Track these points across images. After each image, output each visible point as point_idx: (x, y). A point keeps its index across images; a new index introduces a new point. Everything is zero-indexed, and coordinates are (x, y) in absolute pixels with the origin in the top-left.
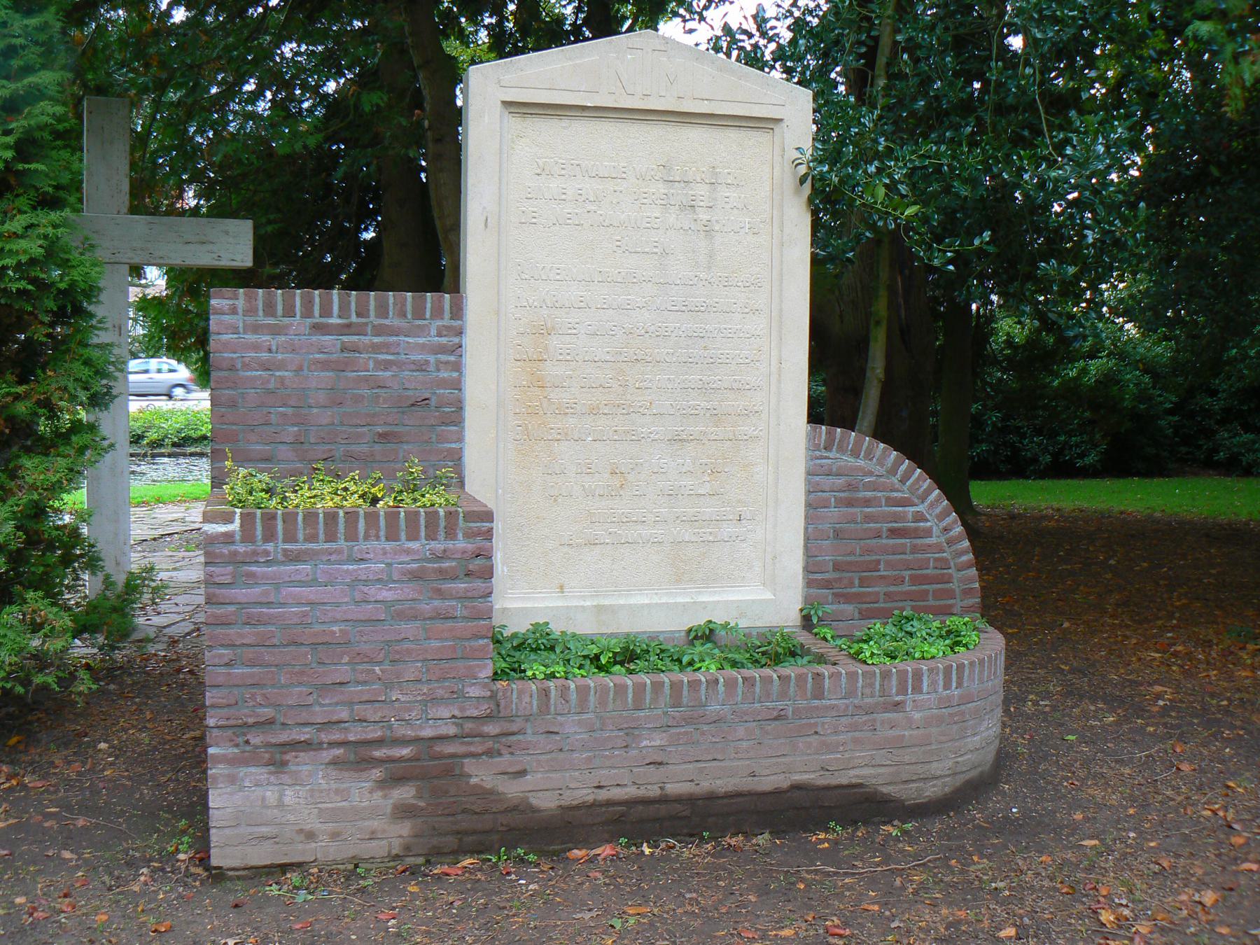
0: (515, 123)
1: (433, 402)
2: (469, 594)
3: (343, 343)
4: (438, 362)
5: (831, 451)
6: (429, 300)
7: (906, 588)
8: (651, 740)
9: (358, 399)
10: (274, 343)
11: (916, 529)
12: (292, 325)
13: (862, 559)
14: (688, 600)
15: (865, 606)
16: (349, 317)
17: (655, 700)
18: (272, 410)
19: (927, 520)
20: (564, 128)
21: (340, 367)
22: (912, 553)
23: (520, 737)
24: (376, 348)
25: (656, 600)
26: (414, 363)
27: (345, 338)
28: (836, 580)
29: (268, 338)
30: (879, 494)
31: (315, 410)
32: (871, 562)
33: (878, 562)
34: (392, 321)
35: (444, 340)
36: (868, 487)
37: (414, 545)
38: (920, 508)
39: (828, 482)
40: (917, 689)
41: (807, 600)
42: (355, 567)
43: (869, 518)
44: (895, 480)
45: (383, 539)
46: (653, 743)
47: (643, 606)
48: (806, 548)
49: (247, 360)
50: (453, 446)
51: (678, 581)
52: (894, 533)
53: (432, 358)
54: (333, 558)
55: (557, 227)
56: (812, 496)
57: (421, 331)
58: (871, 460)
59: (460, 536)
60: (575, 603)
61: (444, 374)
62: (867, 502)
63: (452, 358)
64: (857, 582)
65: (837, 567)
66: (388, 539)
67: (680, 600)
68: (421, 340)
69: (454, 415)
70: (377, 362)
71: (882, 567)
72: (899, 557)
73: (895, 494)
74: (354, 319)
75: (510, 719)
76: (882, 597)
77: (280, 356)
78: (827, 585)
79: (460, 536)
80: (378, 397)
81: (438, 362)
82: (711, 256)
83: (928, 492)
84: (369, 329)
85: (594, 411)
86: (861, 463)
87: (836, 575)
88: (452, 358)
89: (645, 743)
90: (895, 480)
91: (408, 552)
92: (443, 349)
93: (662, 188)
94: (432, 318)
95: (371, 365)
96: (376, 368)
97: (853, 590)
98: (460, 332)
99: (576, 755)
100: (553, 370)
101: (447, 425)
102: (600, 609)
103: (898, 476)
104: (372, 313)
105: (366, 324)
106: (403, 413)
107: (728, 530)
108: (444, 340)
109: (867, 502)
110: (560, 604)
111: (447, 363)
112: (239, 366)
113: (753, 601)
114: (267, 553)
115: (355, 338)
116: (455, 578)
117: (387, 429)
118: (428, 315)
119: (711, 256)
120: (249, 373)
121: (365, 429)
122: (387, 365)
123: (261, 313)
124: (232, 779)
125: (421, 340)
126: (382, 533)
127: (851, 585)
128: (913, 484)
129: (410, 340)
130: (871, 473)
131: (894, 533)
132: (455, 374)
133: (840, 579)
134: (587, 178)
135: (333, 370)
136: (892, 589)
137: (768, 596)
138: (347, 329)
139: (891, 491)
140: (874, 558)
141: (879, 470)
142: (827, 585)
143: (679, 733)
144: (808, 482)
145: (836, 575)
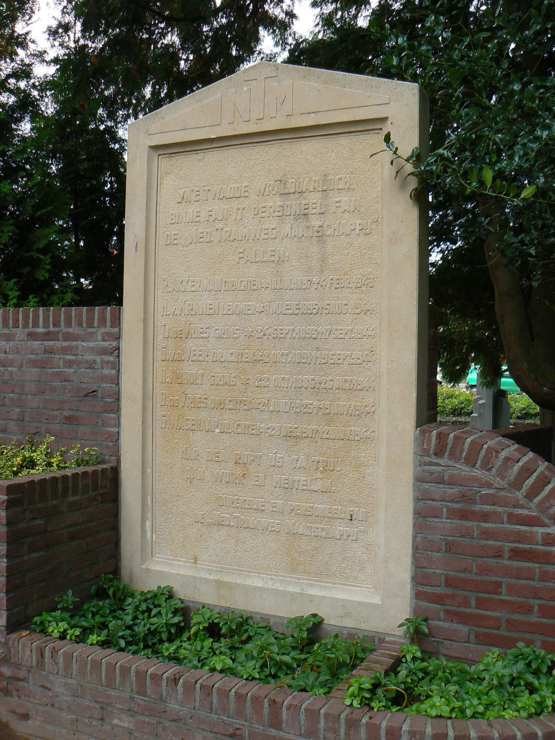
0: (166, 163)
1: (100, 393)
3: (45, 346)
4: (103, 362)
5: (442, 456)
6: (96, 313)
7: (535, 618)
8: (121, 720)
9: (53, 390)
10: (7, 347)
11: (547, 554)
12: (17, 333)
13: (478, 578)
14: (297, 590)
15: (483, 630)
16: (49, 327)
17: (123, 683)
18: (6, 395)
20: (200, 160)
21: (43, 364)
22: (541, 579)
24: (65, 351)
25: (270, 585)
26: (86, 362)
27: (46, 343)
28: (448, 596)
29: (4, 343)
30: (500, 509)
31: (29, 397)
32: (490, 582)
33: (499, 584)
34: (74, 330)
35: (106, 344)
36: (486, 499)
39: (438, 490)
41: (416, 611)
43: (486, 534)
44: (520, 495)
46: (122, 724)
47: (255, 589)
48: (414, 555)
50: (113, 429)
51: (293, 571)
52: (516, 554)
53: (98, 359)
55: (193, 245)
56: (421, 503)
57: (91, 337)
58: (489, 470)
60: (202, 575)
61: (106, 372)
62: (485, 517)
63: (111, 359)
64: (473, 603)
65: (450, 582)
67: (290, 589)
68: (91, 344)
69: (114, 405)
70: (65, 361)
71: (504, 589)
72: (524, 582)
73: (520, 511)
74: (51, 328)
75: (18, 666)
76: (504, 623)
77: (10, 357)
78: (438, 599)
80: (65, 388)
81: (103, 362)
82: (323, 260)
84: (60, 336)
85: (220, 406)
86: (478, 472)
87: (449, 591)
88: (111, 359)
89: (116, 721)
90: (520, 495)
92: (104, 352)
93: (278, 201)
94: (98, 327)
96: (64, 367)
97: (469, 610)
98: (118, 338)
99: (63, 714)
100: (189, 369)
101: (109, 412)
102: (220, 584)
104: (62, 324)
105: (58, 332)
106: (81, 401)
107: (340, 528)
108: (106, 344)
109: (485, 517)
110: (190, 573)
111: (108, 362)
113: (359, 603)
115: (52, 343)
117: (71, 413)
118: (96, 324)
119: (323, 260)
121: (58, 413)
122: (69, 364)
125: (91, 344)
127: (466, 603)
128: (542, 502)
129: (85, 344)
130: (489, 485)
131: (516, 554)
132: (113, 372)
133: (453, 596)
134: (216, 201)
135: (39, 367)
136: (516, 617)
137: (376, 600)
138: (47, 336)
139: (515, 506)
140: (494, 579)
141: (499, 482)
142: (438, 599)
143: (144, 722)
144: (416, 488)
145: (449, 591)
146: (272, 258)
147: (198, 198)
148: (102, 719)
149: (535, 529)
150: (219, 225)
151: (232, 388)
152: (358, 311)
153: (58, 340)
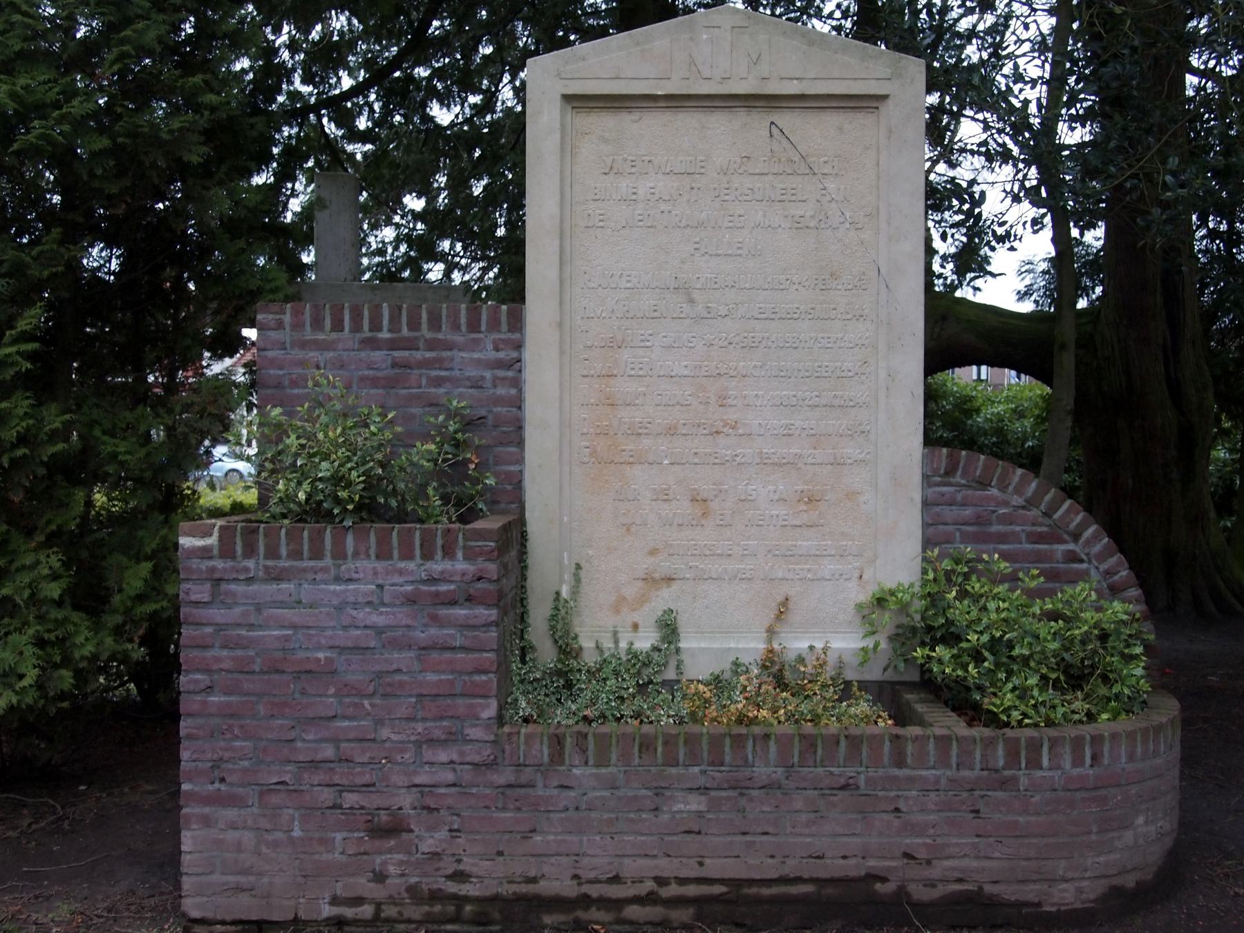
2: (471, 622)
3: (394, 358)
4: (495, 380)
16: (400, 331)
19: (1082, 561)
23: (530, 791)
26: (468, 378)
27: (396, 354)
30: (1018, 529)
36: (1004, 520)
37: (412, 565)
38: (1071, 546)
39: (950, 513)
40: (1035, 763)
42: (343, 587)
45: (373, 557)
49: (294, 376)
50: (512, 468)
53: (488, 375)
54: (318, 577)
56: (931, 530)
57: (475, 345)
59: (460, 555)
61: (501, 391)
66: (378, 557)
68: (476, 355)
70: (429, 378)
79: (460, 555)
83: (1083, 527)
85: (671, 431)
88: (510, 374)
91: (401, 572)
92: (500, 365)
95: (424, 382)
96: (429, 385)
98: (519, 346)
99: (593, 815)
103: (1043, 507)
104: (424, 326)
105: (416, 338)
108: (501, 355)
111: (504, 379)
112: (286, 383)
114: (247, 570)
116: (453, 603)
118: (483, 328)
120: (296, 391)
122: (438, 382)
123: (308, 328)
124: (206, 821)
125: (476, 355)
126: (372, 552)
129: (465, 355)
132: (513, 391)
134: (660, 176)
135: (383, 387)
146: (739, 252)
147: (633, 170)
148: (656, 809)
149: (1056, 547)
150: (663, 207)
151: (685, 408)
152: (849, 317)
153: (418, 349)
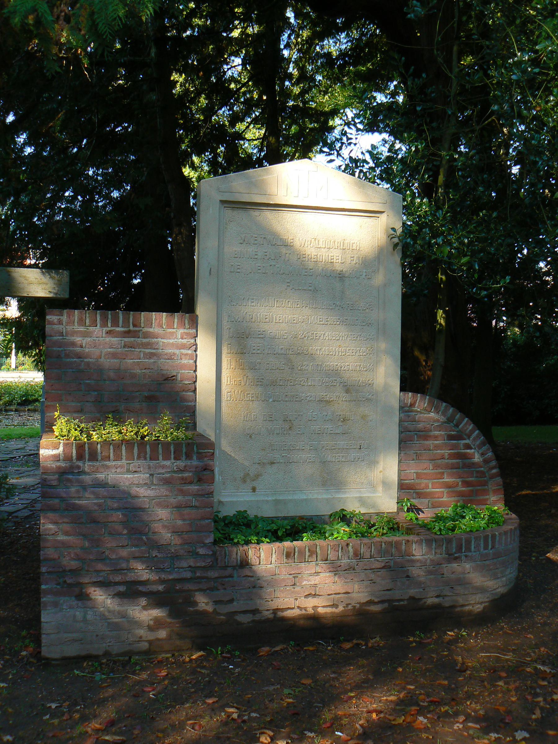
0: (229, 213)
2: (200, 493)
3: (125, 342)
8: (308, 580)
10: (84, 342)
12: (95, 331)
16: (129, 327)
19: (471, 448)
23: (230, 579)
29: (80, 339)
31: (107, 382)
35: (185, 341)
37: (167, 463)
38: (467, 441)
40: (468, 549)
42: (131, 476)
45: (148, 459)
49: (67, 352)
54: (118, 470)
56: (403, 434)
59: (195, 458)
60: (262, 498)
63: (189, 352)
64: (430, 486)
66: (151, 459)
70: (145, 354)
74: (131, 328)
79: (195, 458)
83: (472, 432)
84: (140, 334)
88: (189, 352)
91: (163, 467)
95: (142, 355)
102: (277, 502)
103: (454, 422)
108: (185, 341)
110: (253, 499)
111: (187, 354)
112: (63, 356)
114: (79, 467)
116: (191, 483)
120: (68, 360)
121: (138, 394)
123: (76, 324)
124: (56, 605)
126: (148, 456)
146: (310, 288)
147: (256, 242)
148: (294, 584)
149: (460, 442)
150: (273, 263)
151: (281, 371)
152: (364, 324)
153: (139, 338)
